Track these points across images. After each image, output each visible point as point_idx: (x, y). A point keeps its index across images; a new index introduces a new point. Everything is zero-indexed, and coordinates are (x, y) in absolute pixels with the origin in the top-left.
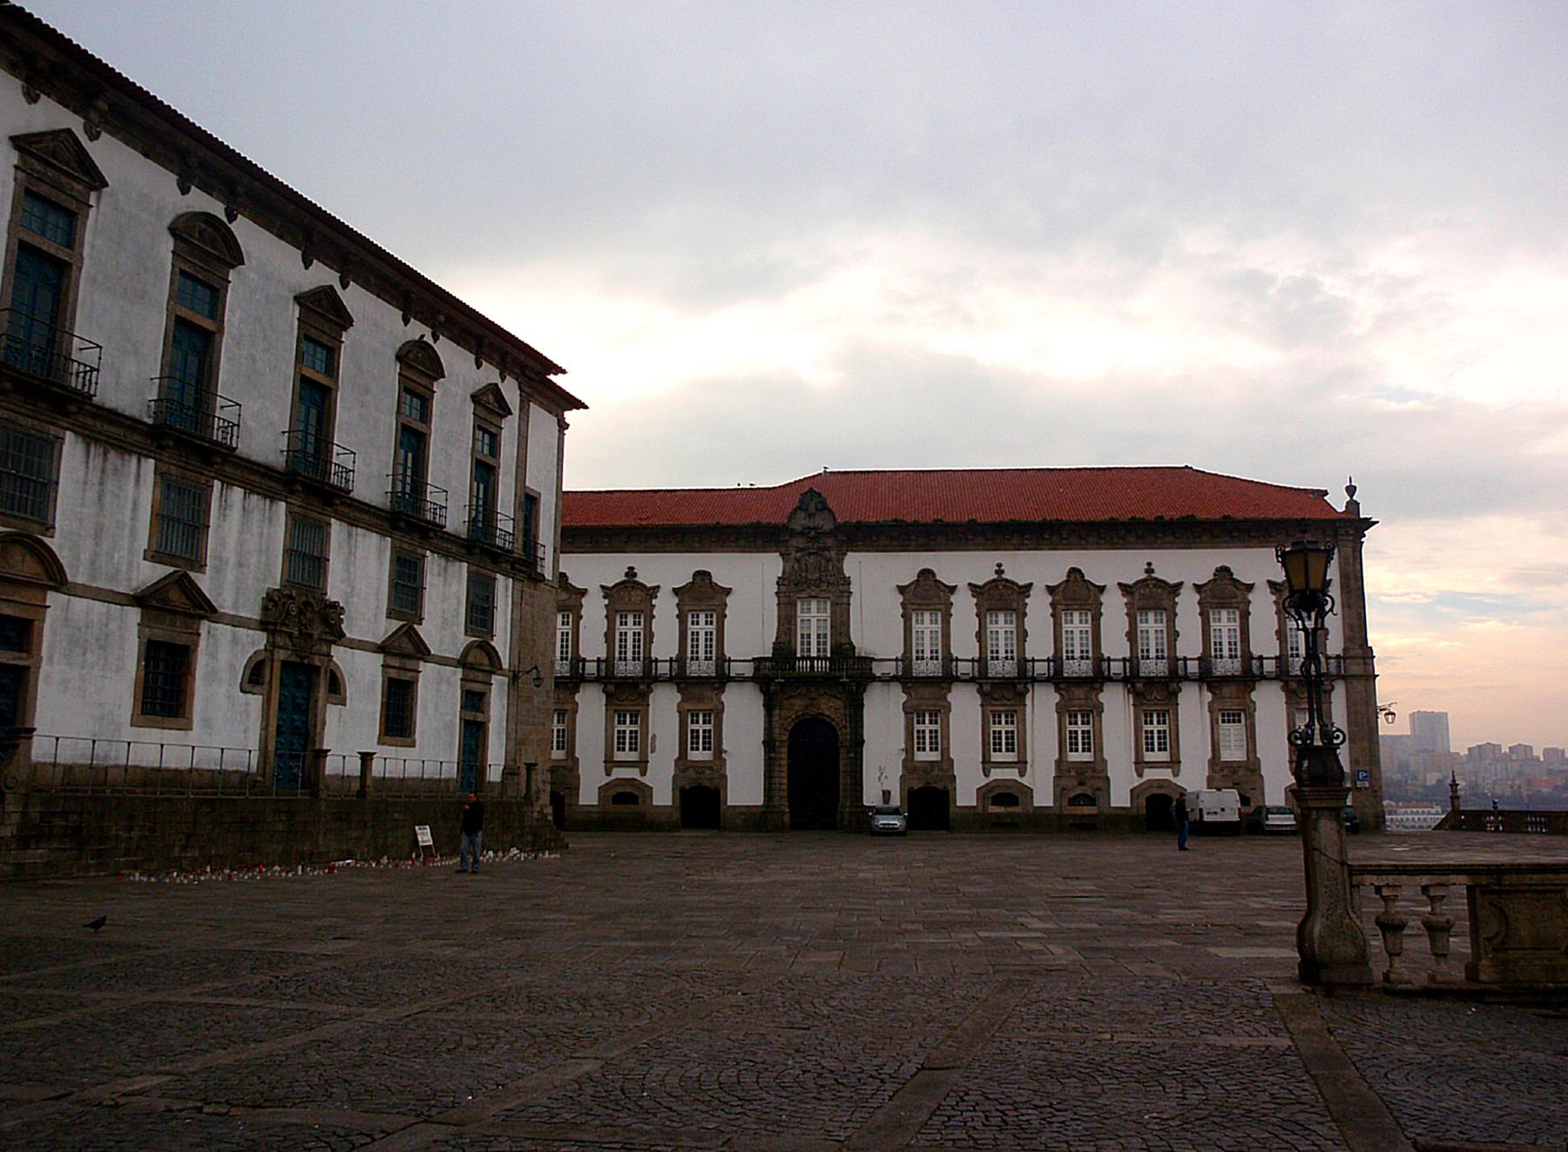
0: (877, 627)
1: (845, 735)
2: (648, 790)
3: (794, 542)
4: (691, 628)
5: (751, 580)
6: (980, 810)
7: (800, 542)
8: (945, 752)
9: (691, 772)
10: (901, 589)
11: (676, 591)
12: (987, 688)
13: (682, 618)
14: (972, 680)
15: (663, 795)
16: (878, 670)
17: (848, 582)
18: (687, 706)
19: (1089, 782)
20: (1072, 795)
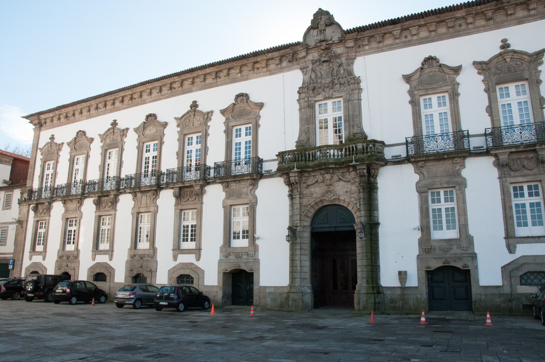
0: (387, 118)
1: (359, 217)
2: (200, 272)
3: (310, 57)
4: (235, 140)
5: (278, 94)
6: (507, 290)
7: (314, 55)
8: (464, 228)
9: (232, 257)
10: (407, 78)
11: (223, 112)
12: (504, 158)
13: (228, 132)
14: (487, 153)
15: (211, 279)
16: (388, 154)
17: (357, 81)
18: (230, 202)
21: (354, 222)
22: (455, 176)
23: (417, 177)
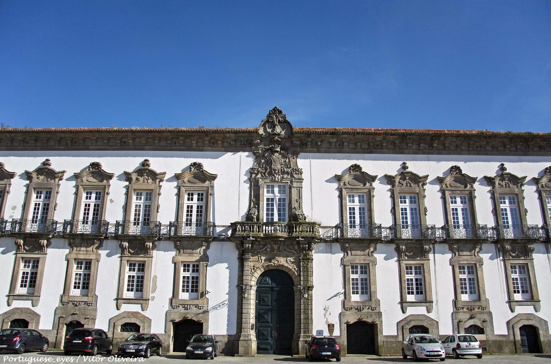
19: (478, 316)
20: (467, 325)
21: (293, 285)
22: (369, 255)
23: (341, 255)
